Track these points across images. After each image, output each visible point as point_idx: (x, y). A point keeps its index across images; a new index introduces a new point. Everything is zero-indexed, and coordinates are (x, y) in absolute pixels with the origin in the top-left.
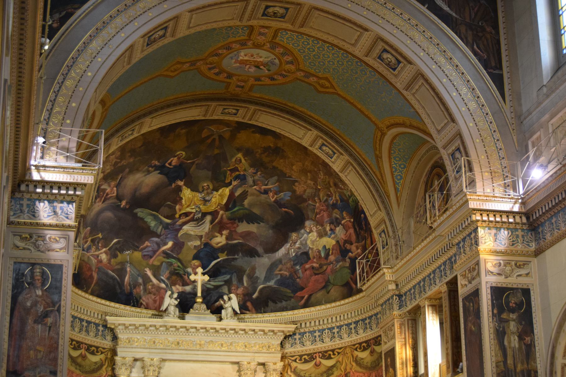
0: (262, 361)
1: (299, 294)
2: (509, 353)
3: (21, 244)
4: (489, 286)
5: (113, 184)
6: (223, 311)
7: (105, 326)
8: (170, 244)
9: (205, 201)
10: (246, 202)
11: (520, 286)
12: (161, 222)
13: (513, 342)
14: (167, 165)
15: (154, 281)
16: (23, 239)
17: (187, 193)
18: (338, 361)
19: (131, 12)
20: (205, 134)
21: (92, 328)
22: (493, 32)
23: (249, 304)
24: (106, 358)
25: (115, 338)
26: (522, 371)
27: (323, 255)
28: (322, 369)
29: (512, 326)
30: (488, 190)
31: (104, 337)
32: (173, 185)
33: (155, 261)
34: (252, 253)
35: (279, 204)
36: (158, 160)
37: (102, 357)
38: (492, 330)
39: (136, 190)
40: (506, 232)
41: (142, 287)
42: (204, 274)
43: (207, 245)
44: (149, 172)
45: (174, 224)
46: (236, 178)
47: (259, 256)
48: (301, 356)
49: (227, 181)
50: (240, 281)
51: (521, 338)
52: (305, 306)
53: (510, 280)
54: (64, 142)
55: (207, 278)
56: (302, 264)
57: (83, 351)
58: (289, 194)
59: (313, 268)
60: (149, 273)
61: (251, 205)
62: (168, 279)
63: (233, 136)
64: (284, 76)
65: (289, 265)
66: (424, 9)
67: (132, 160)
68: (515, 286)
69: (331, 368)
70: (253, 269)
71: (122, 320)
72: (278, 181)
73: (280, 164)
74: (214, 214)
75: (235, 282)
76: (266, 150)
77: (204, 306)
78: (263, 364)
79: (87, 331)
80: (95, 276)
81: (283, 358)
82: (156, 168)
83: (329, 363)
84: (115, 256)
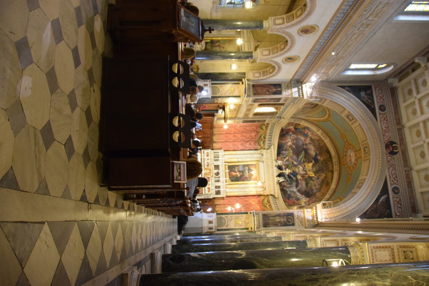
0: (266, 189)
1: (287, 199)
2: (275, 218)
3: (286, 85)
4: (294, 212)
5: (310, 141)
6: (279, 178)
7: (271, 146)
8: (296, 163)
9: (309, 170)
10: (311, 182)
11: (295, 223)
12: (301, 160)
13: (278, 219)
14: (318, 156)
15: (285, 160)
16: (287, 85)
17: (311, 164)
18: (268, 208)
19: (354, 107)
20: (329, 163)
21: (269, 142)
22: (377, 217)
23: (282, 187)
24: (262, 147)
25: (268, 149)
26: (269, 222)
27: (299, 204)
28: (266, 205)
29: (282, 220)
30: (324, 213)
31: (268, 146)
32: (312, 160)
33: (290, 160)
34: (297, 186)
35: (312, 190)
36: (319, 153)
37: (262, 146)
38: (280, 213)
39: (309, 149)
40: (311, 218)
41: (283, 157)
42: (289, 172)
43: (297, 174)
44: (315, 151)
45: (302, 163)
46: (318, 177)
47: (296, 188)
48: (269, 200)
49: (317, 175)
50: (289, 184)
51: (279, 222)
52: (284, 201)
53: (296, 219)
54: (314, 93)
55: (288, 173)
56: (296, 199)
57: (263, 140)
58: (316, 191)
59: (295, 202)
60: (287, 158)
61: (311, 183)
62: (286, 164)
63: (329, 171)
64: (349, 169)
65: (295, 196)
66: (378, 193)
67: (317, 144)
68: (295, 221)
69: (266, 207)
70: (292, 187)
71: (273, 150)
72: (319, 188)
73: (324, 187)
74: (306, 174)
75: (288, 183)
76: (328, 181)
77: (280, 173)
78: (265, 189)
79: (269, 140)
80: (284, 142)
81: (268, 195)
82: (316, 153)
83: (268, 206)
84: (290, 147)
